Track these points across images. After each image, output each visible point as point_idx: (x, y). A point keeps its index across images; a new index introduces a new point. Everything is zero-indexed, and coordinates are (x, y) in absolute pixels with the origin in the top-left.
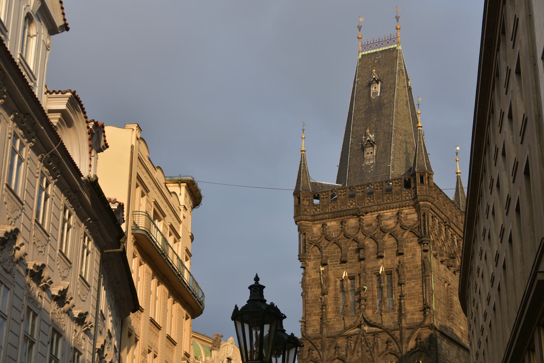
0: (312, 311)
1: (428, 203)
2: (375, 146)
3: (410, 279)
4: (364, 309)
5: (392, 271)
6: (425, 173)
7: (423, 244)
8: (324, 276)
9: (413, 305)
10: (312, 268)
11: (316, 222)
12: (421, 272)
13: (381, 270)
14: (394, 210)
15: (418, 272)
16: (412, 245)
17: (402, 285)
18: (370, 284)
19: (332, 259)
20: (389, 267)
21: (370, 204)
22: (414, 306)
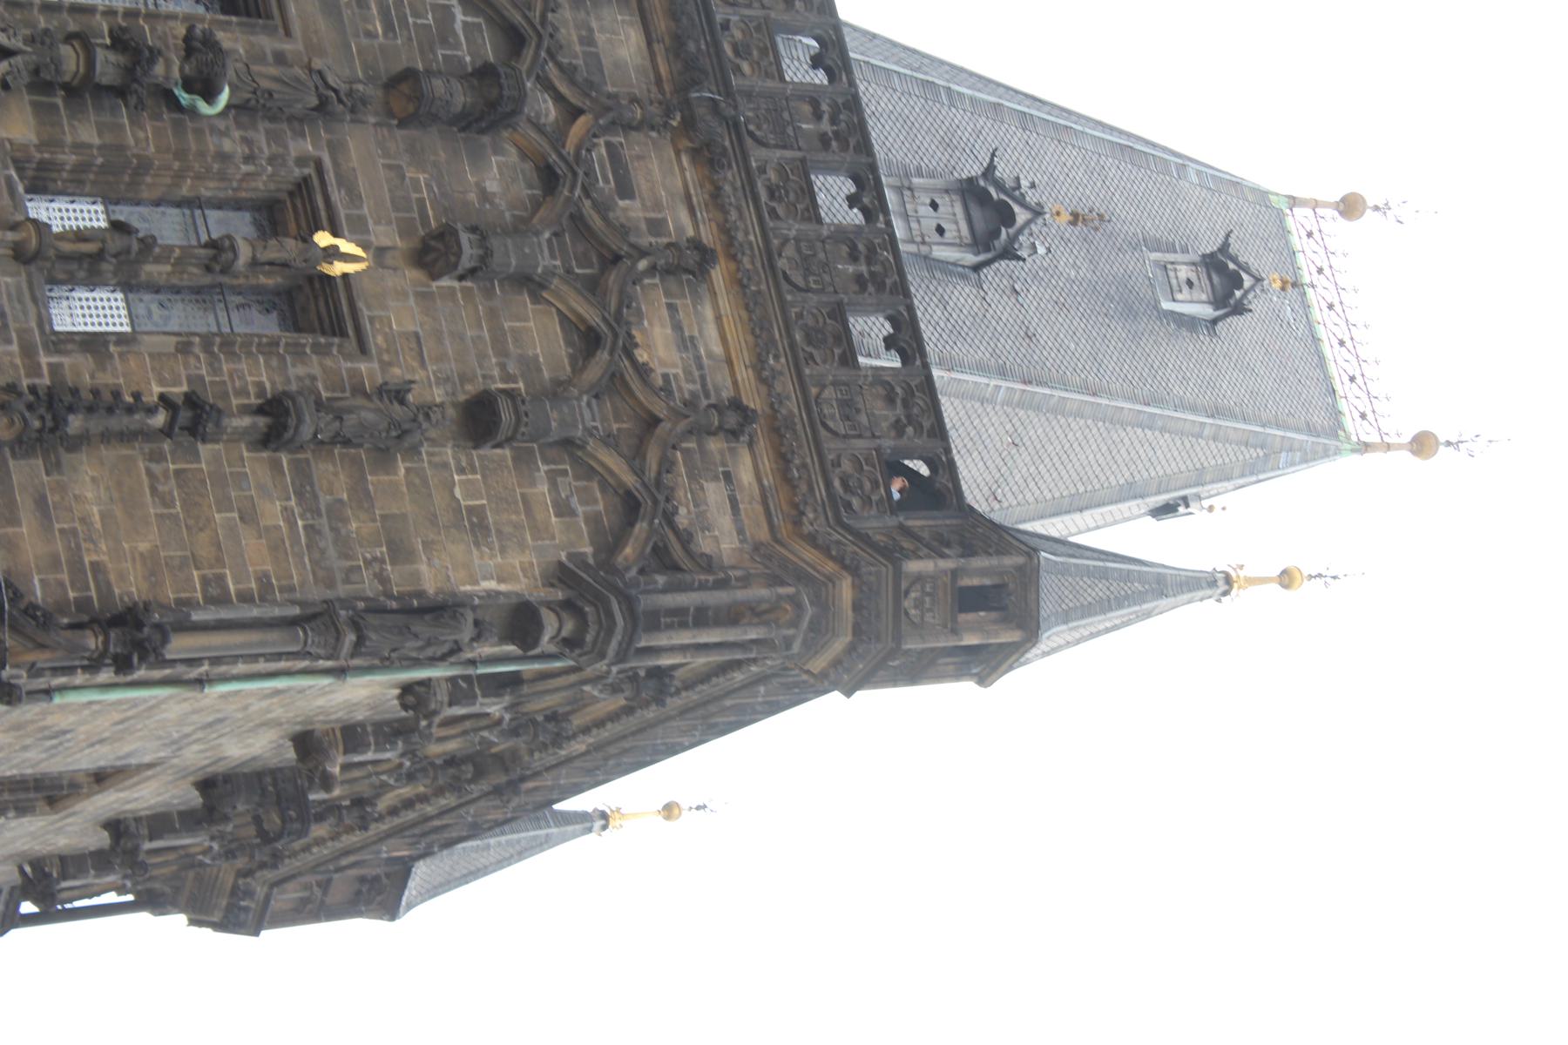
1: (839, 645)
2: (970, 258)
3: (304, 488)
4: (41, 83)
5: (343, 334)
6: (1020, 626)
7: (568, 605)
9: (119, 513)
12: (368, 585)
13: (346, 246)
14: (744, 375)
15: (368, 563)
16: (540, 516)
17: (262, 422)
18: (227, 145)
20: (365, 313)
21: (764, 196)
22: (103, 516)
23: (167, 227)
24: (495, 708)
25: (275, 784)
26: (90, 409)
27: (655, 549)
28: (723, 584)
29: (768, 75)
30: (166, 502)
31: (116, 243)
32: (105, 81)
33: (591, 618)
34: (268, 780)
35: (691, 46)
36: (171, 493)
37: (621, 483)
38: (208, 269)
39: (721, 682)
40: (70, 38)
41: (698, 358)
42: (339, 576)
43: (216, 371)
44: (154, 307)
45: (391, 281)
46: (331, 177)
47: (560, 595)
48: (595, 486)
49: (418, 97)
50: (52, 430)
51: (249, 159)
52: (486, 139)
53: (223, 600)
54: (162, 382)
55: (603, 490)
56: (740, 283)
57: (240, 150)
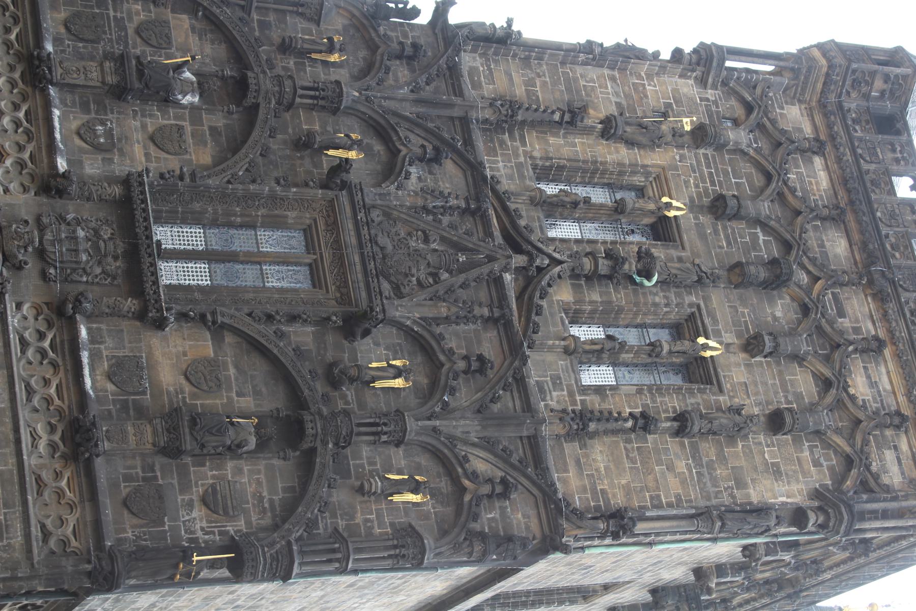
0: (539, 76)
3: (695, 454)
4: (575, 275)
5: (711, 383)
7: (820, 508)
8: (664, 127)
9: (612, 467)
10: (675, 91)
11: (818, 118)
12: (726, 500)
13: (712, 343)
14: (902, 399)
15: (726, 489)
16: (806, 467)
17: (676, 424)
18: (657, 299)
19: (715, 162)
21: (908, 315)
22: (606, 468)
23: (631, 337)
24: (787, 557)
25: (685, 592)
26: (599, 420)
27: (861, 482)
28: (895, 499)
29: (908, 258)
30: (634, 462)
31: (608, 345)
32: (603, 273)
33: (832, 515)
34: (682, 590)
35: (871, 246)
36: (635, 457)
37: (844, 451)
38: (650, 355)
39: (896, 546)
40: (587, 255)
41: (879, 391)
42: (712, 495)
43: (654, 402)
44: (626, 373)
45: (733, 359)
46: (704, 312)
47: (816, 504)
48: (831, 452)
49: (743, 274)
50: (583, 430)
51: (667, 305)
52: (775, 292)
53: (659, 506)
54: (630, 407)
55: (835, 455)
56: (898, 356)
57: (663, 301)
